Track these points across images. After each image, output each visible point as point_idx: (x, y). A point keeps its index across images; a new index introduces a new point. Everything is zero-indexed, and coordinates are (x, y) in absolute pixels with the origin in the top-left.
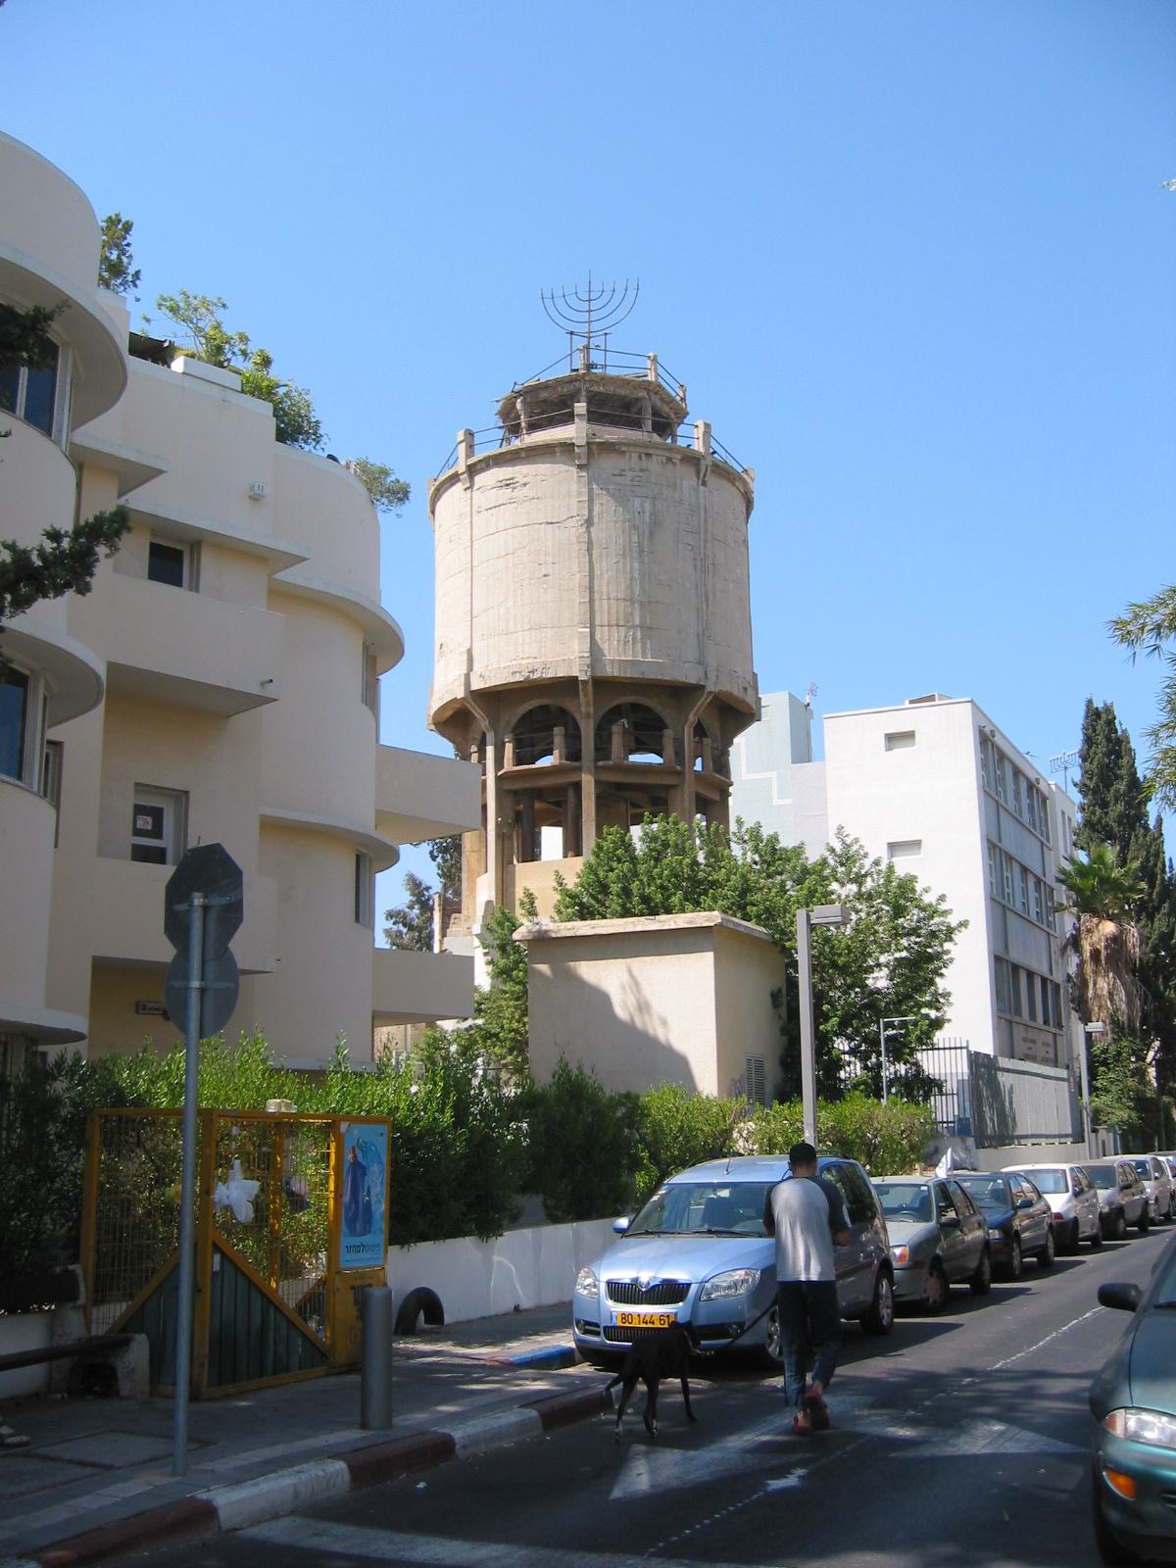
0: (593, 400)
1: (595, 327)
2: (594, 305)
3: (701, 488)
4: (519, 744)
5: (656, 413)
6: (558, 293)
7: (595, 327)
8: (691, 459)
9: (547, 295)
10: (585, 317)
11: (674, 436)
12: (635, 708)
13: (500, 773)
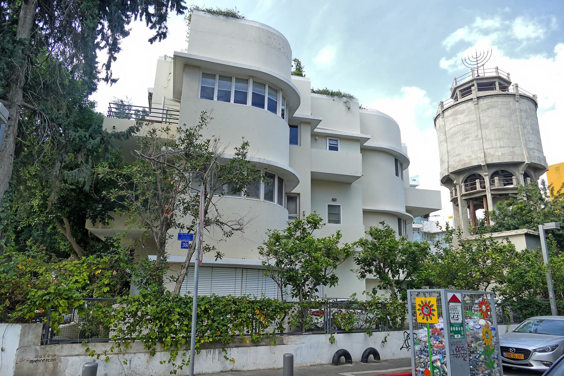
0: (479, 85)
1: (479, 65)
2: (478, 59)
4: (466, 186)
5: (500, 84)
6: (467, 58)
8: (513, 95)
11: (508, 91)
12: (503, 171)
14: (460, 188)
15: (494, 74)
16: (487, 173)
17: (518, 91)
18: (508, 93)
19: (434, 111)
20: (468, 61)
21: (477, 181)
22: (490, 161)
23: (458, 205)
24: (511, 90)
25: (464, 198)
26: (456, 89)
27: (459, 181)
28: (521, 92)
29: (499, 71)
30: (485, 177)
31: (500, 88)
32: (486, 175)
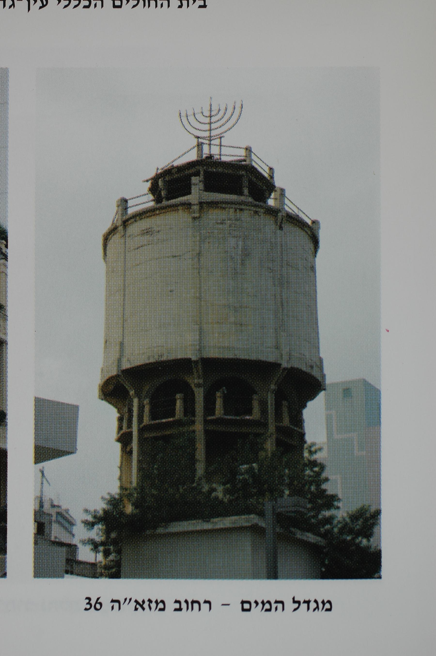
1: (213, 133)
2: (213, 119)
3: (278, 231)
6: (190, 113)
7: (213, 133)
8: (273, 212)
9: (183, 114)
10: (207, 127)
14: (141, 408)
16: (201, 381)
19: (108, 217)
20: (191, 119)
23: (131, 452)
29: (253, 157)
30: (196, 390)
31: (251, 194)
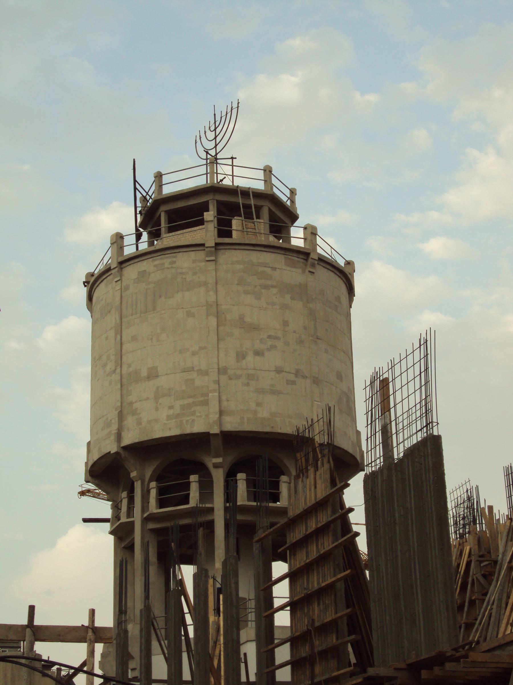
4: (161, 491)
13: (145, 515)
15: (260, 186)
17: (315, 245)
18: (285, 246)
21: (194, 478)
22: (231, 424)
23: (131, 548)
24: (297, 237)
25: (151, 526)
26: (158, 203)
27: (143, 476)
28: (323, 249)
32: (216, 466)
